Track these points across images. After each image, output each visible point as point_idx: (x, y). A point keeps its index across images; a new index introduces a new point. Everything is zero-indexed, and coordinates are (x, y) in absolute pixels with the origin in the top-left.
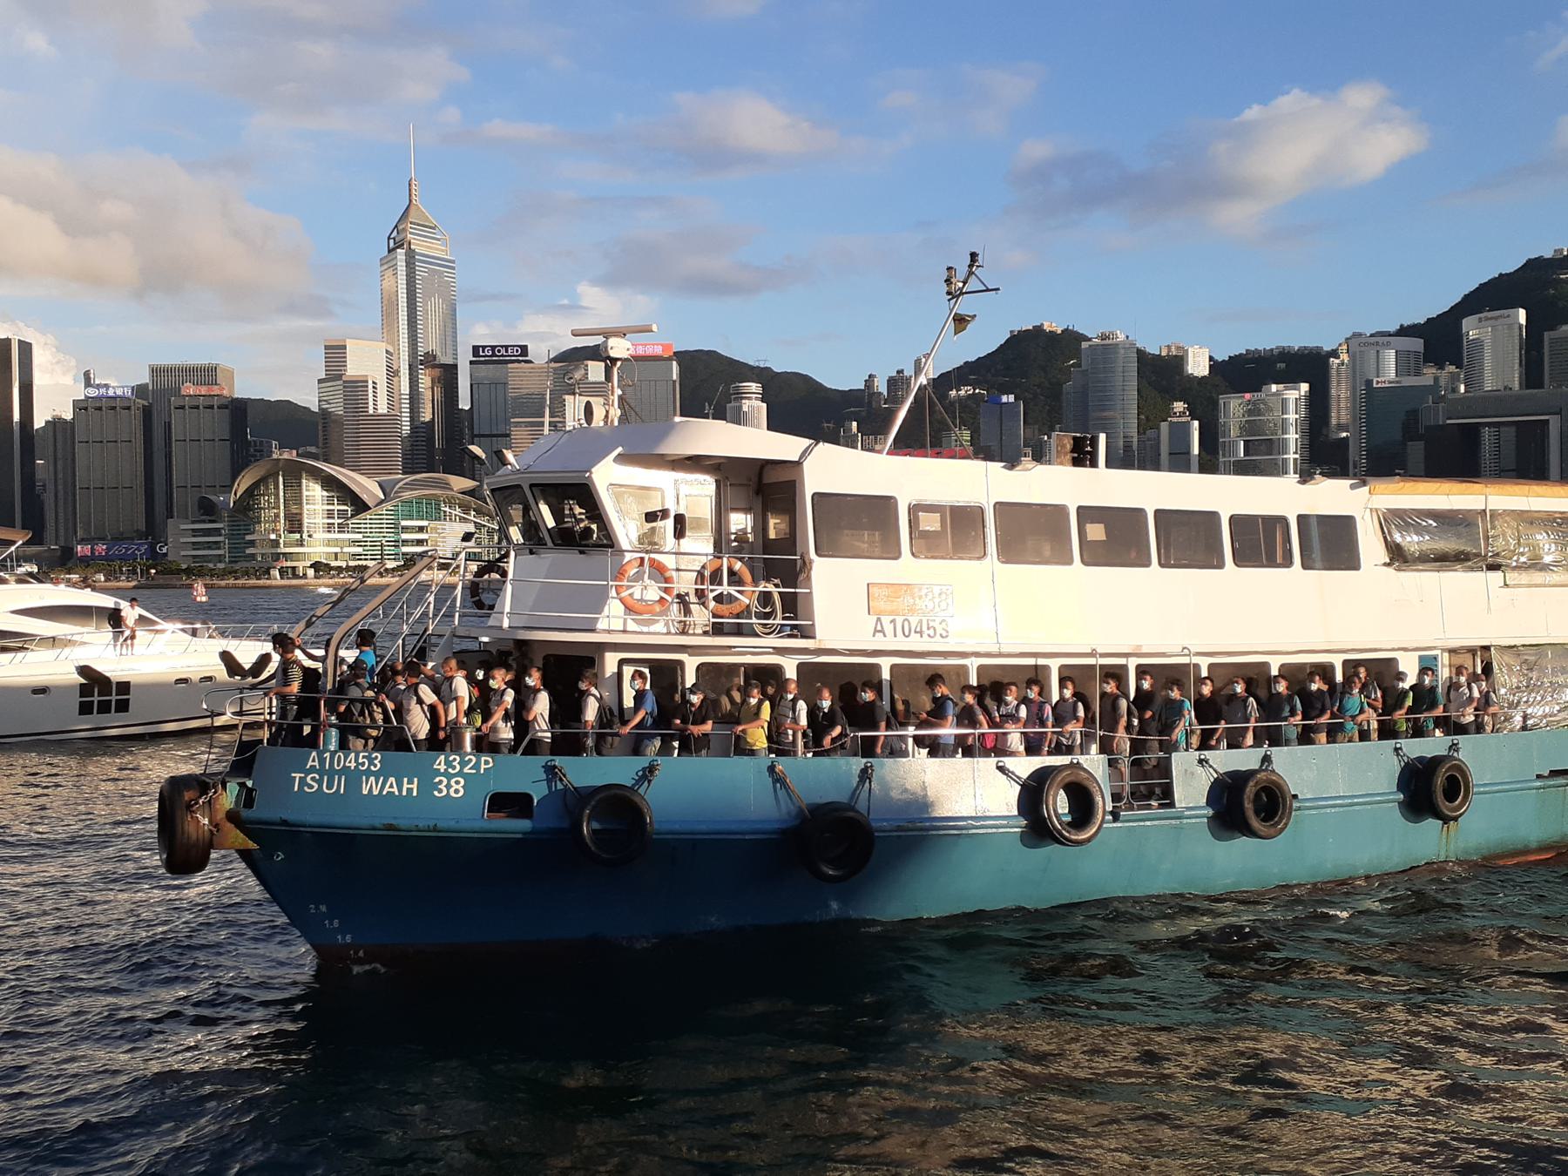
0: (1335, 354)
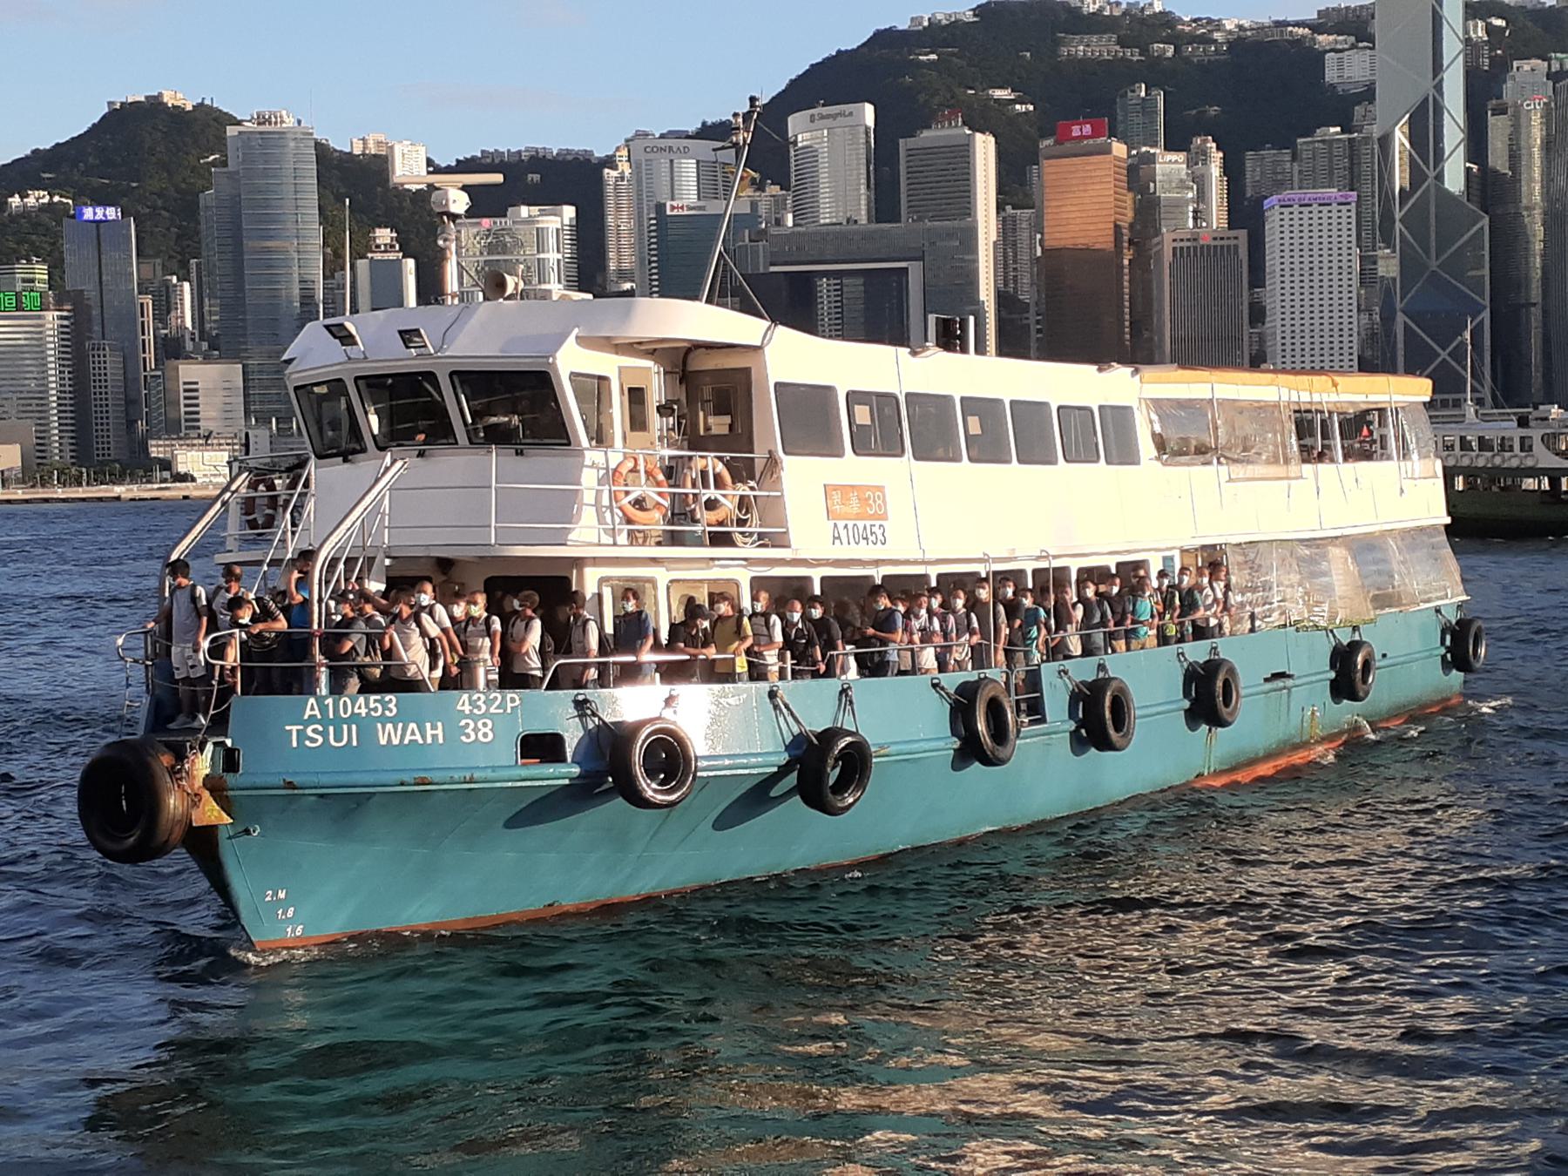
0: (610, 162)
